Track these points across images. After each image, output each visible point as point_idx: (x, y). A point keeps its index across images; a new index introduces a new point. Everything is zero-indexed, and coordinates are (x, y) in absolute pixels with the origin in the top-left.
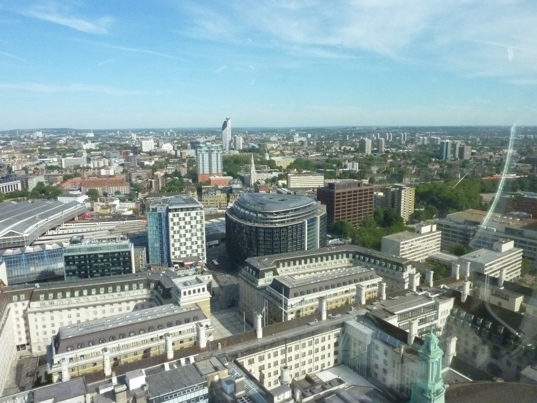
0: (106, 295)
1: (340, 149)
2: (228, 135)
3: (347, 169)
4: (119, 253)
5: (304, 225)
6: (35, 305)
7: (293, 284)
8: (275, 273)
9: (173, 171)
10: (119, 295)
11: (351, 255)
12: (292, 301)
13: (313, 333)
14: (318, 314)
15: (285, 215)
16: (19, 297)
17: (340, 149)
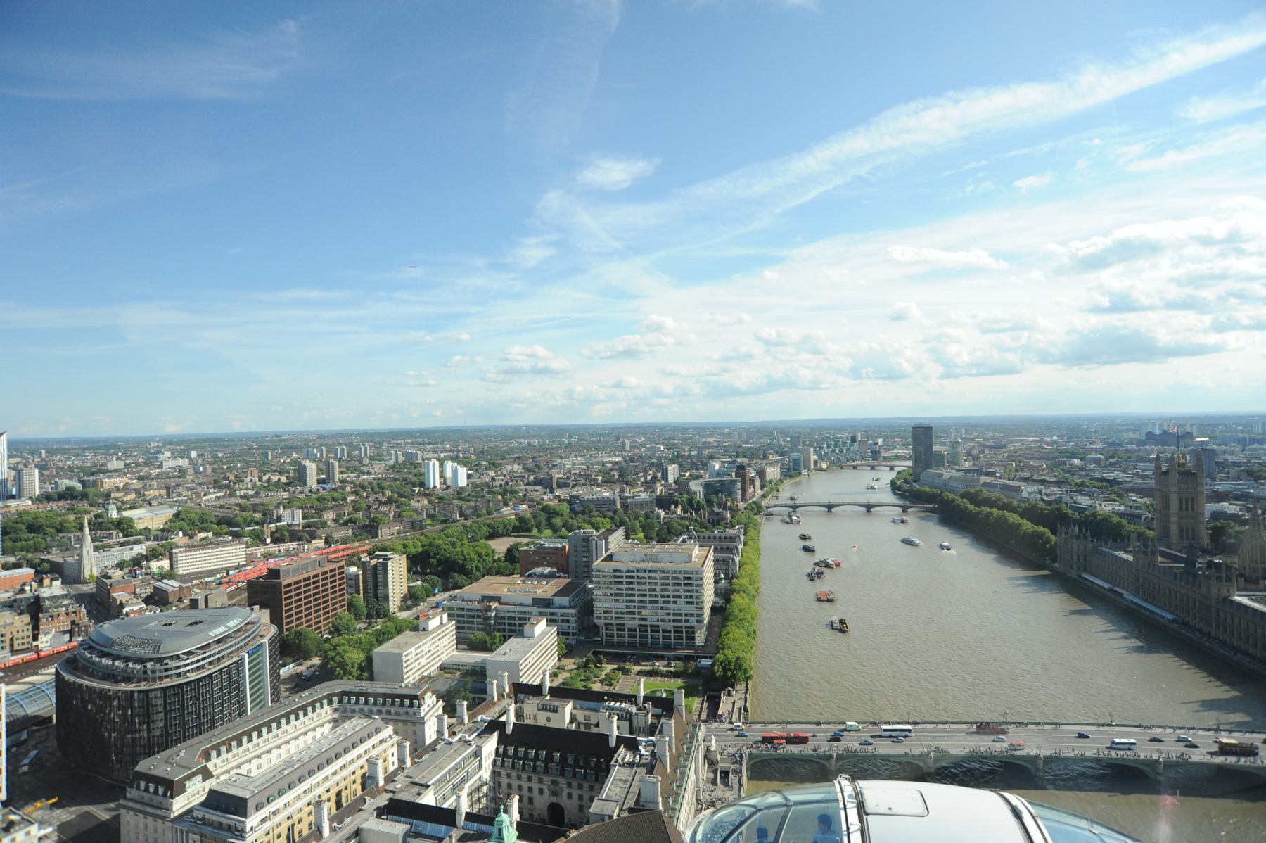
3: (282, 523)
5: (243, 663)
7: (250, 787)
8: (207, 774)
11: (335, 699)
15: (205, 653)
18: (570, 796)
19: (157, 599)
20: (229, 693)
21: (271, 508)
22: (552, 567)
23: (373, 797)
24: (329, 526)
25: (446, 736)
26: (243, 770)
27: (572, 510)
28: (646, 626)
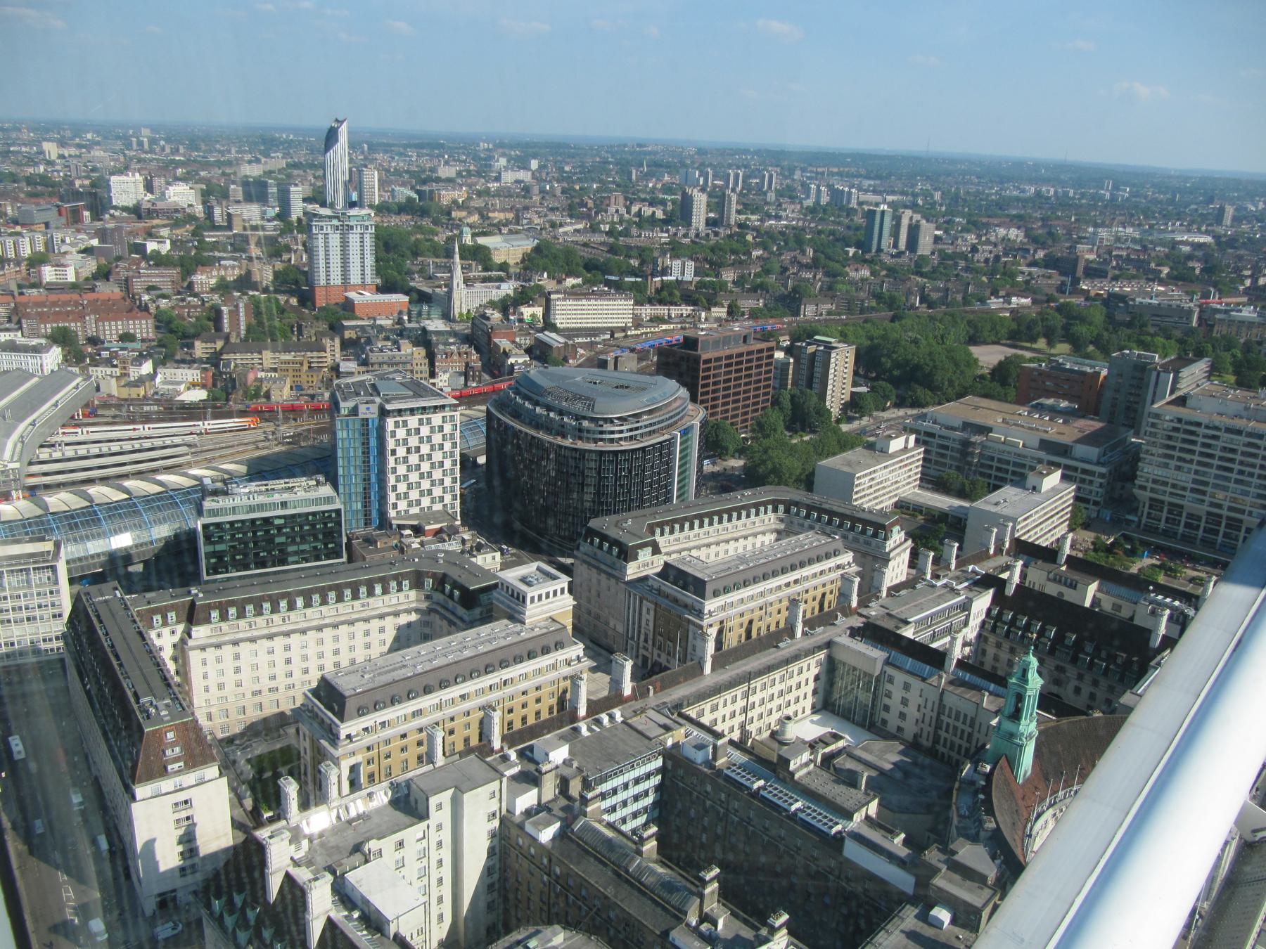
0: (340, 605)
1: (629, 212)
2: (340, 160)
3: (670, 278)
4: (314, 514)
6: (201, 633)
7: (707, 571)
8: (656, 550)
9: (237, 272)
10: (363, 605)
11: (781, 507)
12: (710, 605)
13: (787, 661)
14: (790, 630)
16: (165, 618)
17: (629, 212)
18: (1077, 690)
19: (539, 352)
20: (659, 474)
21: (656, 254)
22: (1070, 402)
23: (845, 615)
24: (731, 292)
25: (928, 577)
26: (694, 553)
27: (1110, 318)
28: (1220, 516)
